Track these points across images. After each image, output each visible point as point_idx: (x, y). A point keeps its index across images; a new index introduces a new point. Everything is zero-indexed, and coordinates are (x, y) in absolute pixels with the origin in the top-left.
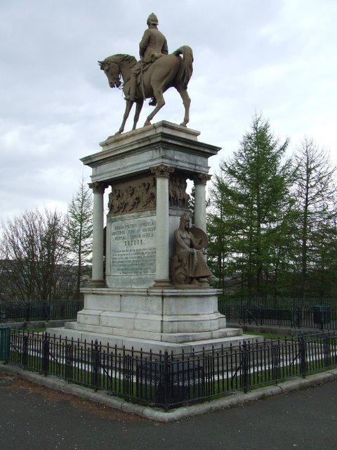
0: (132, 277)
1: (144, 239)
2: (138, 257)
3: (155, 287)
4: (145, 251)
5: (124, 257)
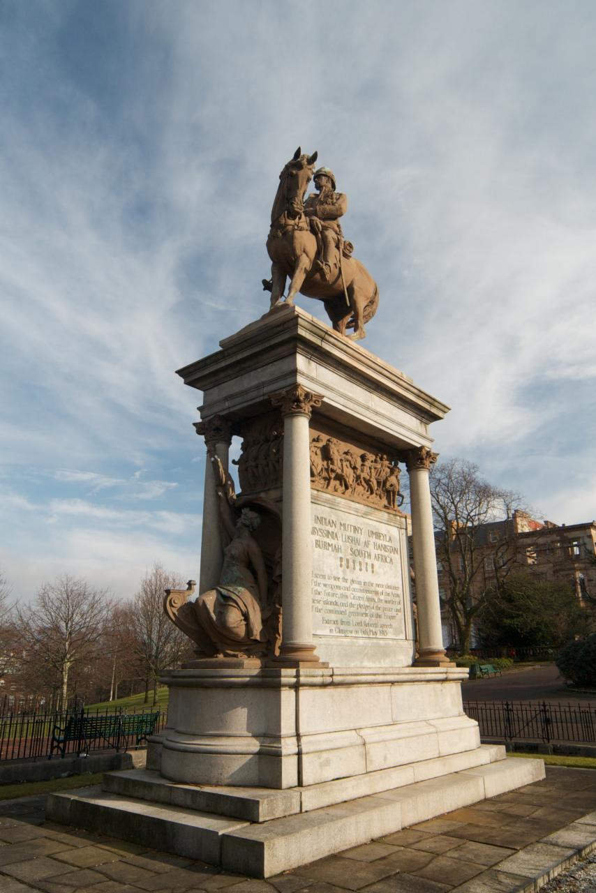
0: (361, 642)
1: (377, 564)
2: (369, 600)
4: (380, 590)
5: (339, 592)
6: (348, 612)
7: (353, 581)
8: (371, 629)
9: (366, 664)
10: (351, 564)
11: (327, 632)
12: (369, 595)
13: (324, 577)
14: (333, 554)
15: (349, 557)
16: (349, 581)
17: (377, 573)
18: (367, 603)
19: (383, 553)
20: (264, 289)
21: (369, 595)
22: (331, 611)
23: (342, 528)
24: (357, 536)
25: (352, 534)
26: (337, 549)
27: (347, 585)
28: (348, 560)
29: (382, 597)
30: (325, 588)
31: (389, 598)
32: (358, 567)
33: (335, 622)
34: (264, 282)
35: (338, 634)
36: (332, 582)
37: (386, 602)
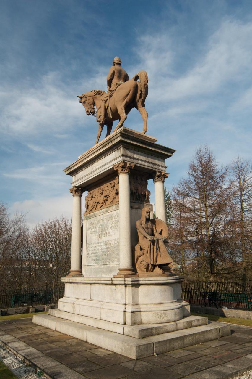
0: (103, 266)
2: (107, 248)
3: (119, 275)
4: (111, 242)
9: (103, 275)
10: (101, 235)
11: (92, 264)
14: (95, 234)
17: (111, 235)
22: (93, 256)
27: (99, 245)
29: (113, 246)
30: (92, 248)
32: (103, 236)
33: (95, 260)
35: (96, 265)
36: (94, 245)
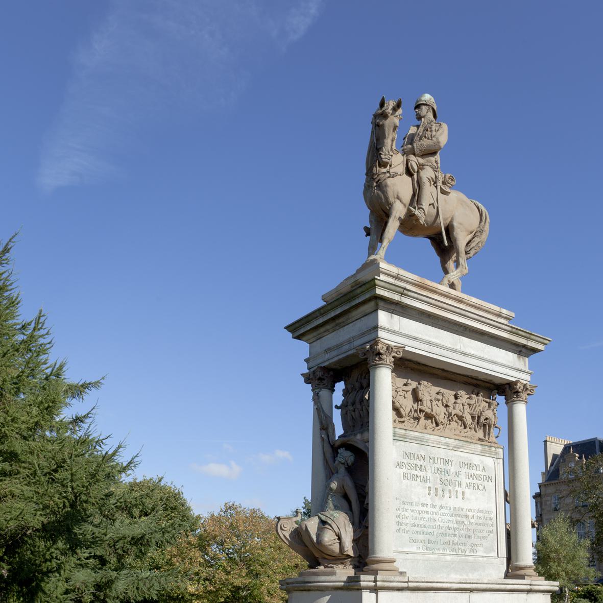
0: (448, 558)
1: (467, 491)
2: (457, 522)
6: (435, 533)
7: (442, 507)
8: (460, 547)
10: (440, 492)
11: (414, 549)
12: (459, 519)
13: (411, 504)
15: (438, 486)
16: (437, 507)
17: (468, 499)
18: (456, 526)
19: (475, 481)
20: (366, 236)
21: (459, 519)
22: (418, 532)
23: (431, 461)
24: (448, 467)
25: (442, 466)
26: (425, 480)
27: (434, 510)
28: (436, 489)
29: (472, 520)
30: (412, 513)
31: (481, 521)
32: (447, 495)
34: (366, 229)
35: (426, 551)
37: (477, 524)
